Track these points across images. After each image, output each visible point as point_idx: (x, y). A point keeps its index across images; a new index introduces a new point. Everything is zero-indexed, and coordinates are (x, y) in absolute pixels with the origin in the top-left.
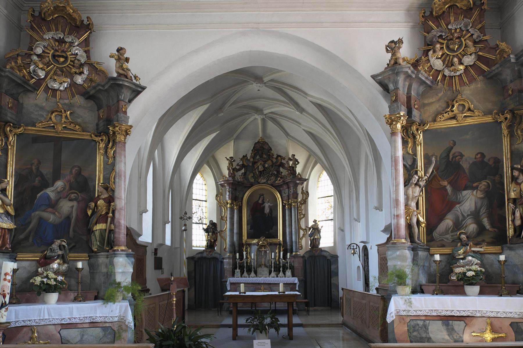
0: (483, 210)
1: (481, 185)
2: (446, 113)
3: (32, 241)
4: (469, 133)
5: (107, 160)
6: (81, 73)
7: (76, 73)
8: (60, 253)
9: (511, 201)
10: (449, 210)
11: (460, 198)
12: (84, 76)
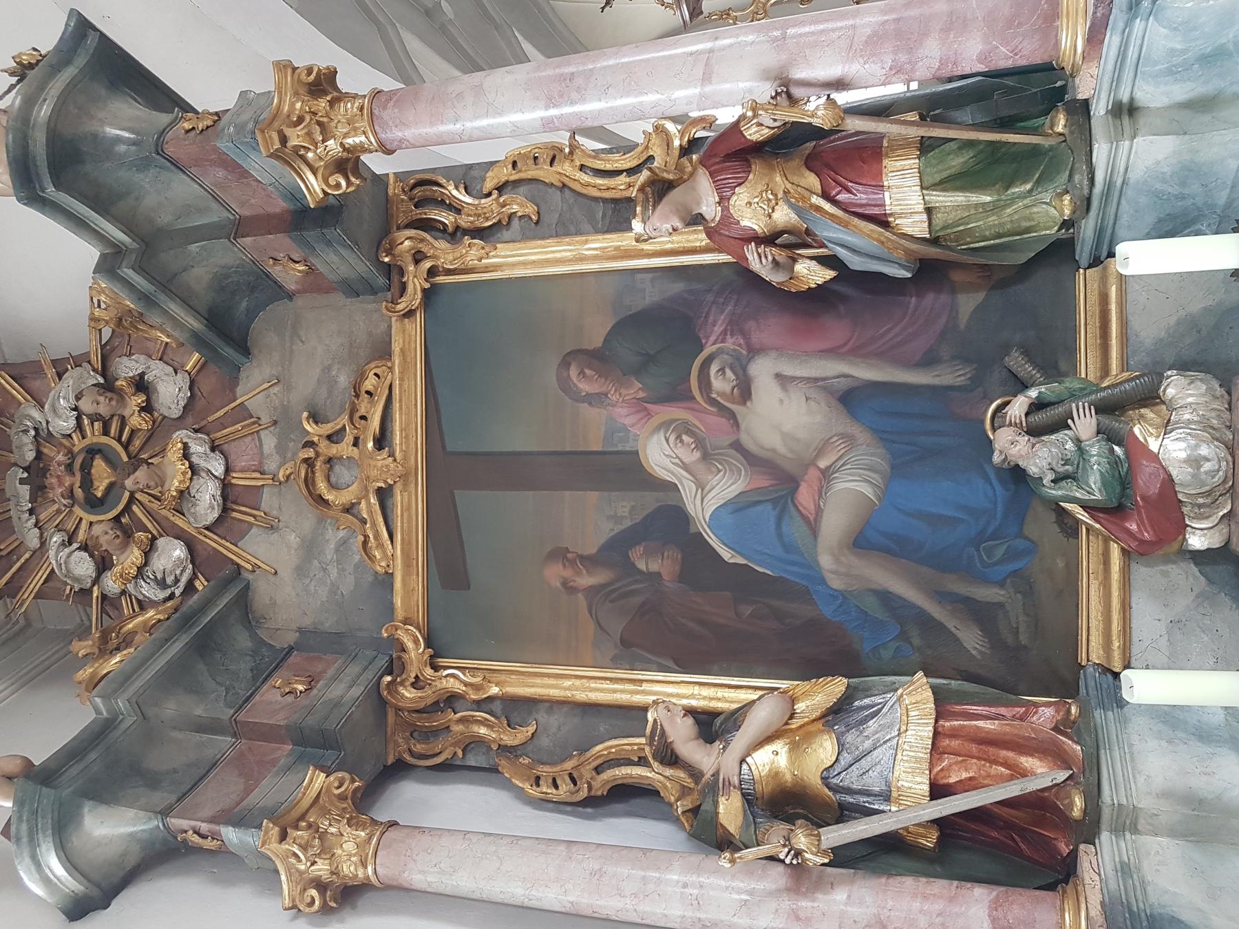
3: (1001, 584)
5: (515, 222)
6: (141, 384)
7: (147, 408)
8: (1085, 424)
12: (157, 372)
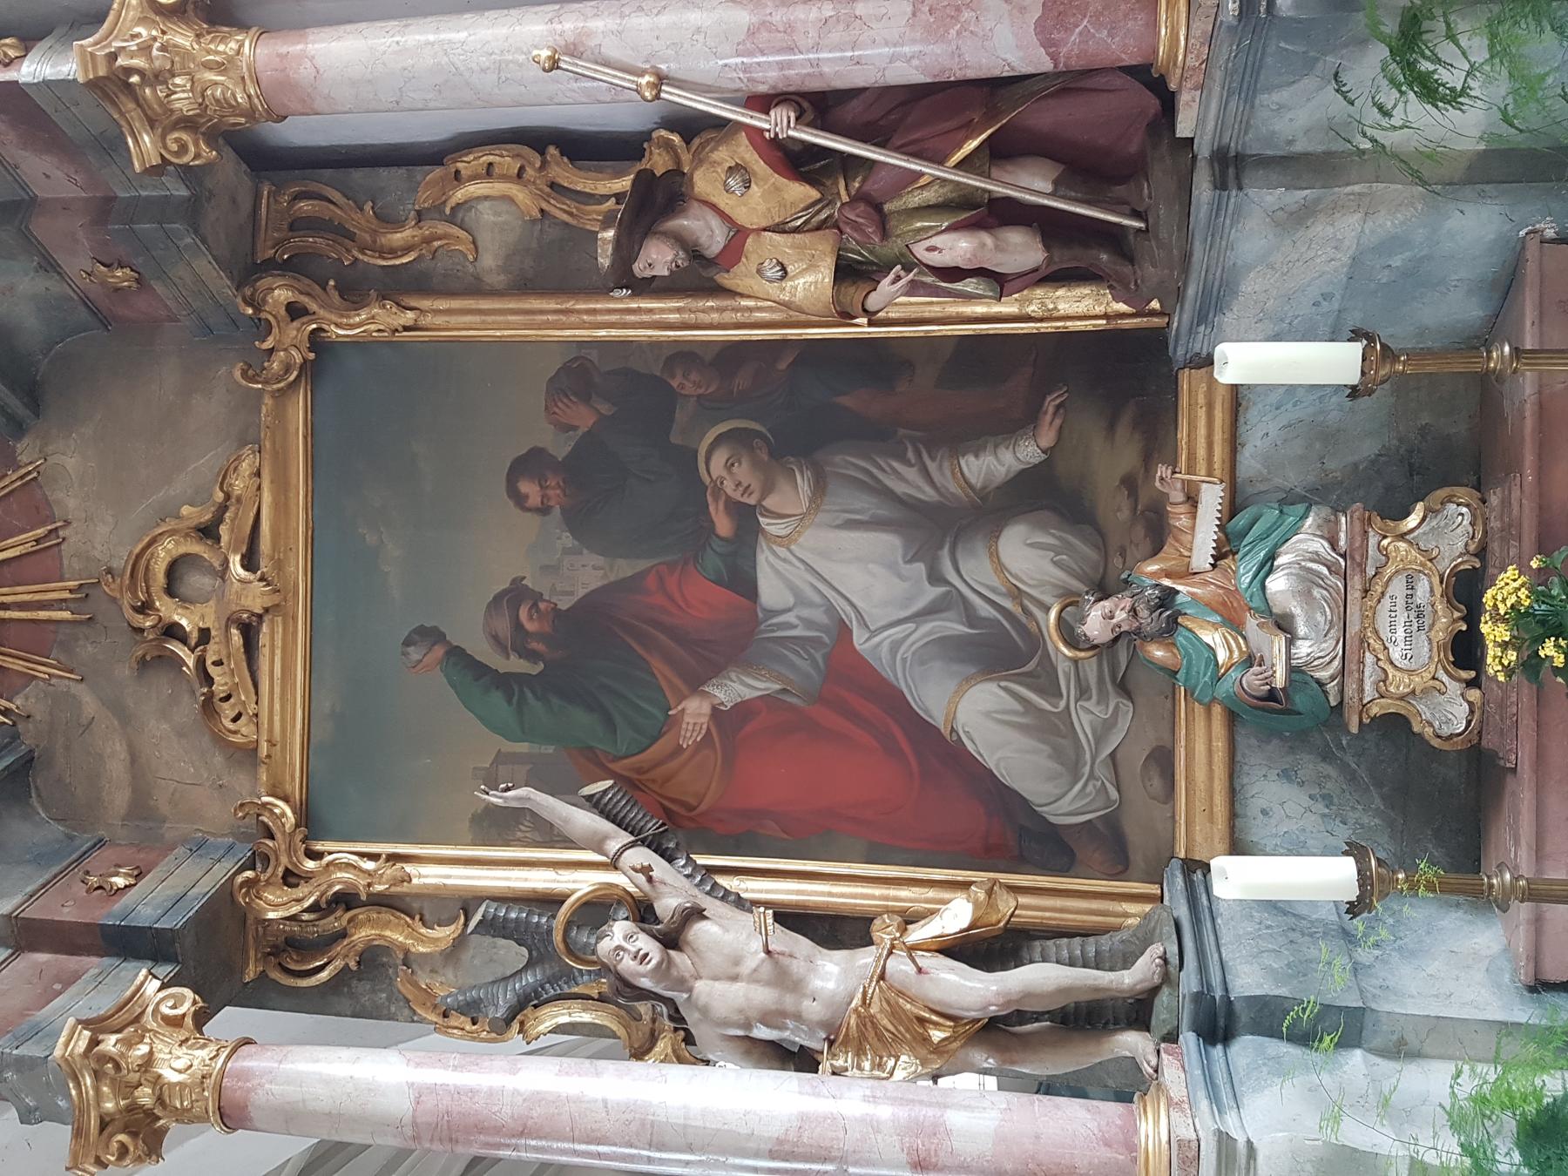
0: (907, 480)
1: (729, 486)
2: (209, 680)
4: (371, 539)
9: (853, 294)
10: (893, 702)
11: (809, 623)
